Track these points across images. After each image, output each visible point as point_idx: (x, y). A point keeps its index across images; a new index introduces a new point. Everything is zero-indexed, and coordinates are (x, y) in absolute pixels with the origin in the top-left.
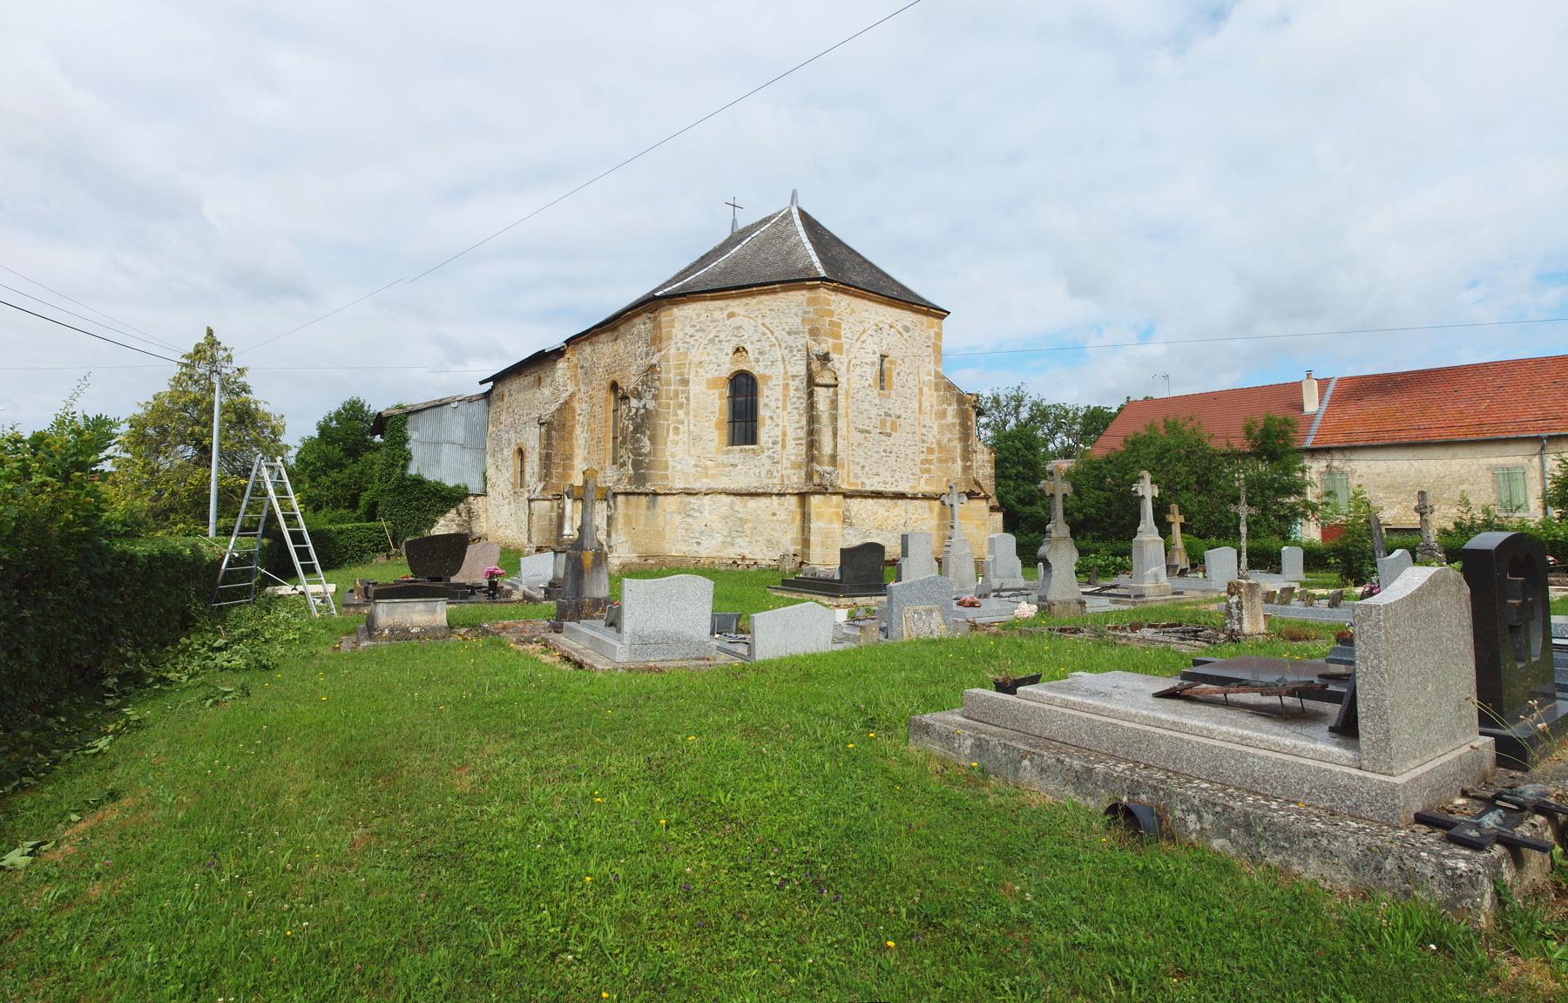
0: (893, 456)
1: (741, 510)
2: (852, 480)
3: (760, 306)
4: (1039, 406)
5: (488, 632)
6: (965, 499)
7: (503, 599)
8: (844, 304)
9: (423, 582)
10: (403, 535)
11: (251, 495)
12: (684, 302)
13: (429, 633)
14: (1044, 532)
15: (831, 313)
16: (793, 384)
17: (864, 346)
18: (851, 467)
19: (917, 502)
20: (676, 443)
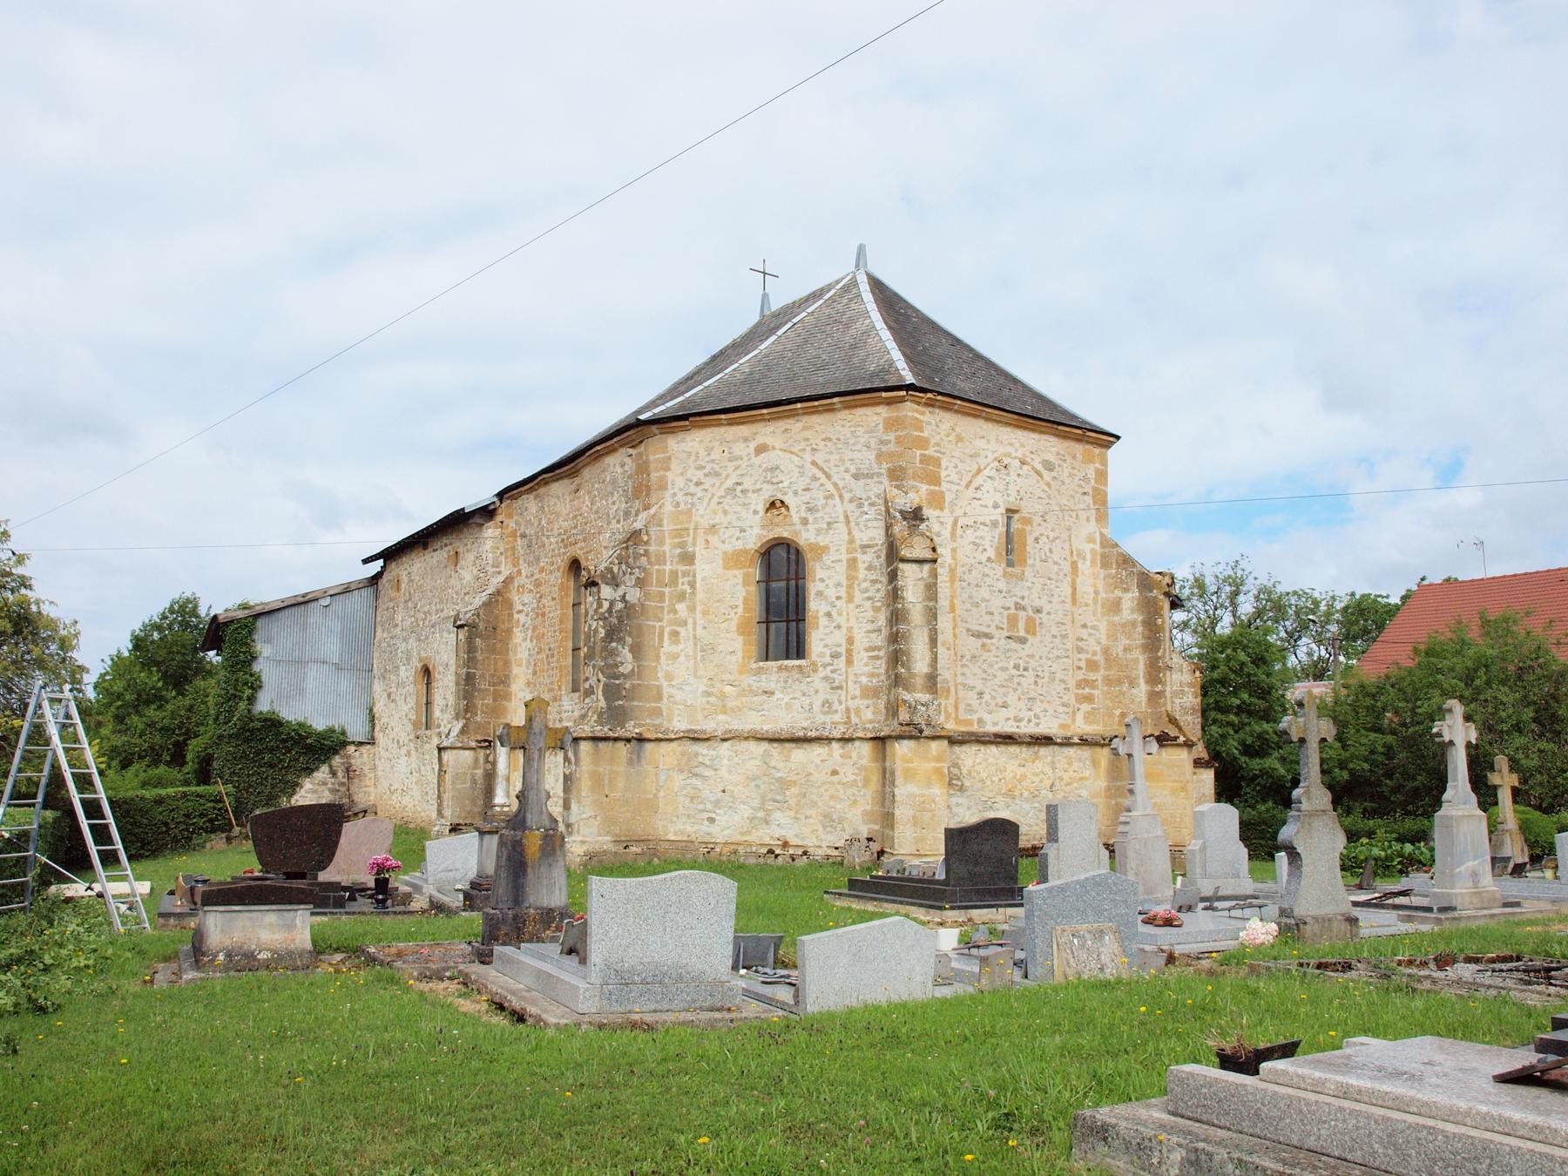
0: (1030, 674)
1: (781, 765)
2: (961, 717)
3: (808, 434)
4: (1270, 593)
5: (374, 960)
6: (1154, 746)
7: (398, 909)
8: (945, 427)
9: (276, 880)
10: (250, 806)
11: (27, 743)
12: (685, 429)
13: (284, 960)
14: (1287, 803)
15: (923, 443)
16: (865, 559)
18: (962, 694)
19: (1071, 751)
20: (675, 657)
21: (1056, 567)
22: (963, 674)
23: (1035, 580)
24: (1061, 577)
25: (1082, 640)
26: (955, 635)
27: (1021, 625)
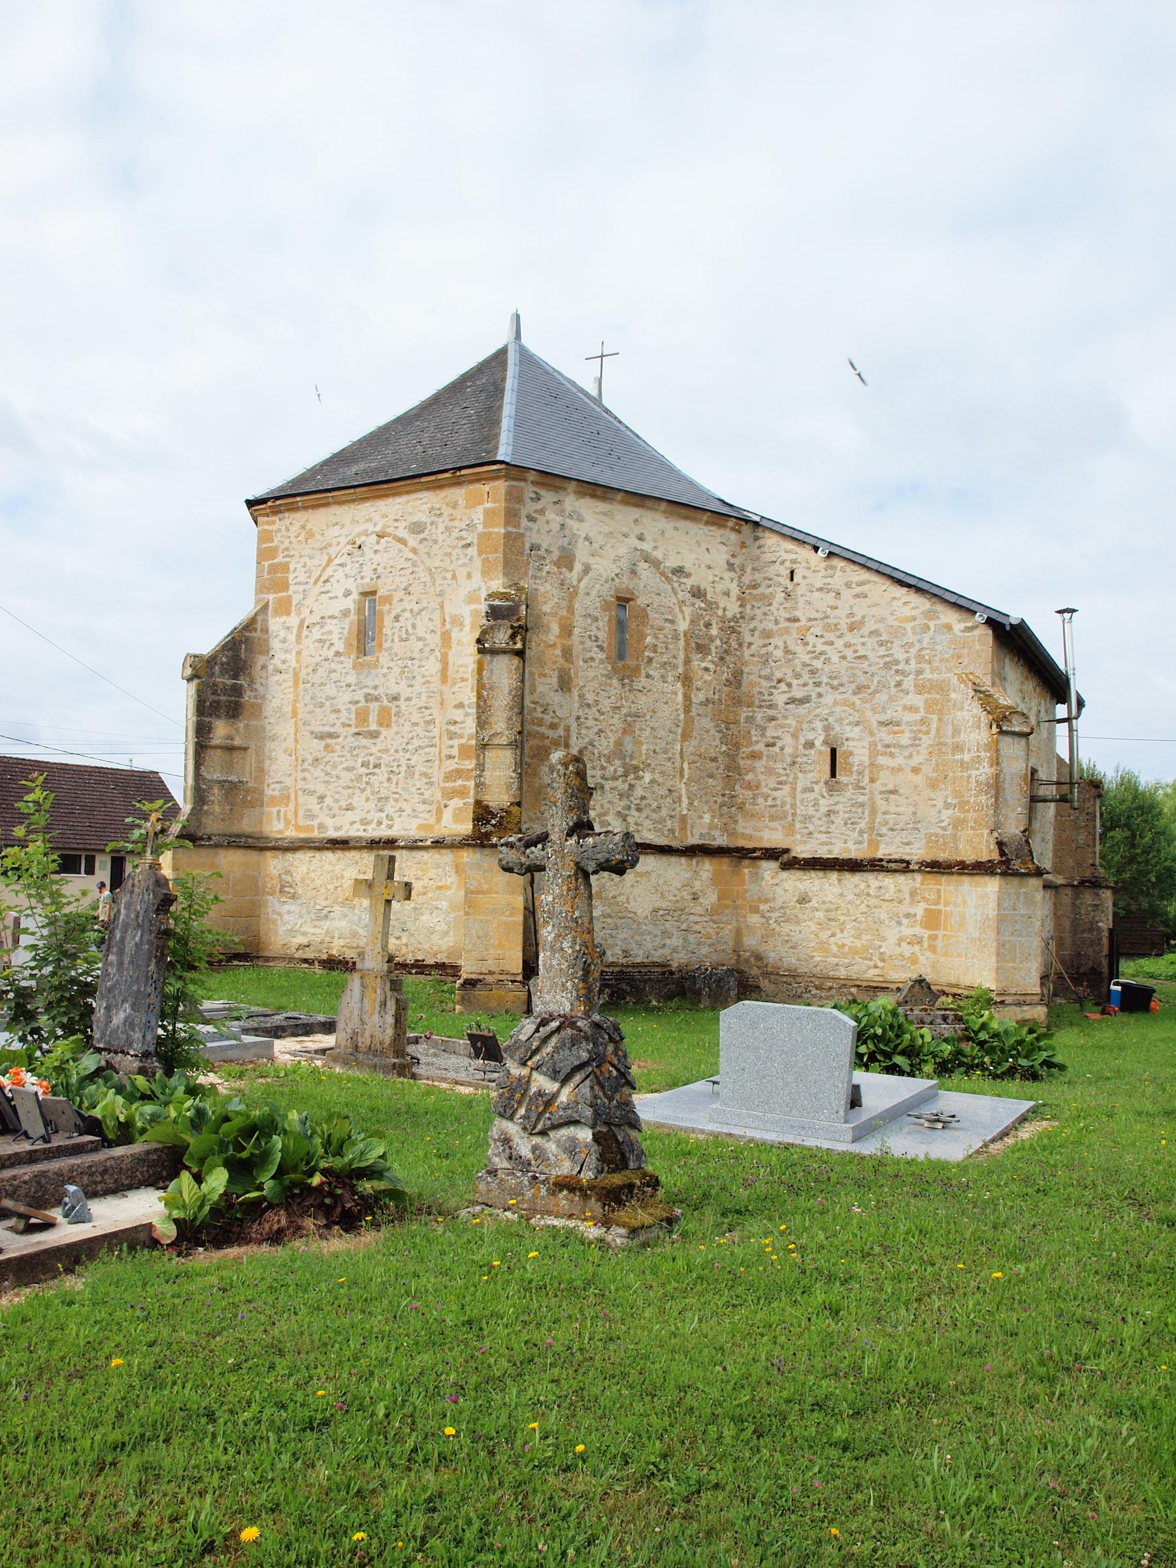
2: (301, 823)
8: (295, 529)
17: (328, 587)
18: (302, 799)
19: (425, 856)
21: (420, 644)
22: (304, 779)
23: (392, 664)
24: (426, 654)
25: (456, 722)
26: (296, 740)
27: (373, 718)
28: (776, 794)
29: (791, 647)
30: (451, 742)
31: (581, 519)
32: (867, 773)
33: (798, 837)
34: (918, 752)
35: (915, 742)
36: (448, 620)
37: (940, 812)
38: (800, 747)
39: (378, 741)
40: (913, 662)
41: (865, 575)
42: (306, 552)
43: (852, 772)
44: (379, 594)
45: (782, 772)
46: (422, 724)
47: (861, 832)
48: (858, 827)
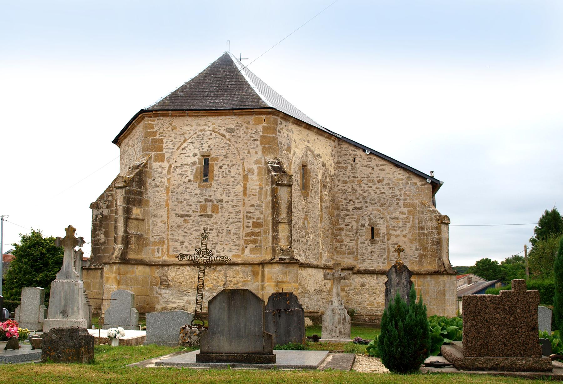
2: (171, 254)
17: (184, 151)
18: (171, 243)
21: (233, 179)
23: (218, 187)
25: (250, 212)
26: (168, 217)
28: (350, 244)
29: (355, 187)
30: (248, 221)
31: (293, 133)
32: (386, 237)
33: (359, 261)
34: (405, 230)
35: (404, 226)
36: (246, 170)
37: (414, 252)
38: (359, 226)
39: (212, 219)
40: (402, 196)
41: (383, 162)
42: (173, 135)
43: (380, 237)
44: (211, 156)
45: (352, 236)
46: (234, 212)
47: (385, 259)
48: (383, 257)
